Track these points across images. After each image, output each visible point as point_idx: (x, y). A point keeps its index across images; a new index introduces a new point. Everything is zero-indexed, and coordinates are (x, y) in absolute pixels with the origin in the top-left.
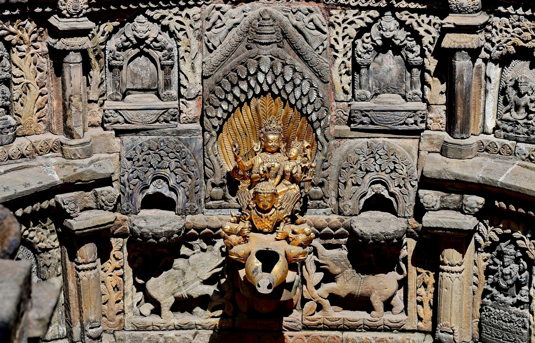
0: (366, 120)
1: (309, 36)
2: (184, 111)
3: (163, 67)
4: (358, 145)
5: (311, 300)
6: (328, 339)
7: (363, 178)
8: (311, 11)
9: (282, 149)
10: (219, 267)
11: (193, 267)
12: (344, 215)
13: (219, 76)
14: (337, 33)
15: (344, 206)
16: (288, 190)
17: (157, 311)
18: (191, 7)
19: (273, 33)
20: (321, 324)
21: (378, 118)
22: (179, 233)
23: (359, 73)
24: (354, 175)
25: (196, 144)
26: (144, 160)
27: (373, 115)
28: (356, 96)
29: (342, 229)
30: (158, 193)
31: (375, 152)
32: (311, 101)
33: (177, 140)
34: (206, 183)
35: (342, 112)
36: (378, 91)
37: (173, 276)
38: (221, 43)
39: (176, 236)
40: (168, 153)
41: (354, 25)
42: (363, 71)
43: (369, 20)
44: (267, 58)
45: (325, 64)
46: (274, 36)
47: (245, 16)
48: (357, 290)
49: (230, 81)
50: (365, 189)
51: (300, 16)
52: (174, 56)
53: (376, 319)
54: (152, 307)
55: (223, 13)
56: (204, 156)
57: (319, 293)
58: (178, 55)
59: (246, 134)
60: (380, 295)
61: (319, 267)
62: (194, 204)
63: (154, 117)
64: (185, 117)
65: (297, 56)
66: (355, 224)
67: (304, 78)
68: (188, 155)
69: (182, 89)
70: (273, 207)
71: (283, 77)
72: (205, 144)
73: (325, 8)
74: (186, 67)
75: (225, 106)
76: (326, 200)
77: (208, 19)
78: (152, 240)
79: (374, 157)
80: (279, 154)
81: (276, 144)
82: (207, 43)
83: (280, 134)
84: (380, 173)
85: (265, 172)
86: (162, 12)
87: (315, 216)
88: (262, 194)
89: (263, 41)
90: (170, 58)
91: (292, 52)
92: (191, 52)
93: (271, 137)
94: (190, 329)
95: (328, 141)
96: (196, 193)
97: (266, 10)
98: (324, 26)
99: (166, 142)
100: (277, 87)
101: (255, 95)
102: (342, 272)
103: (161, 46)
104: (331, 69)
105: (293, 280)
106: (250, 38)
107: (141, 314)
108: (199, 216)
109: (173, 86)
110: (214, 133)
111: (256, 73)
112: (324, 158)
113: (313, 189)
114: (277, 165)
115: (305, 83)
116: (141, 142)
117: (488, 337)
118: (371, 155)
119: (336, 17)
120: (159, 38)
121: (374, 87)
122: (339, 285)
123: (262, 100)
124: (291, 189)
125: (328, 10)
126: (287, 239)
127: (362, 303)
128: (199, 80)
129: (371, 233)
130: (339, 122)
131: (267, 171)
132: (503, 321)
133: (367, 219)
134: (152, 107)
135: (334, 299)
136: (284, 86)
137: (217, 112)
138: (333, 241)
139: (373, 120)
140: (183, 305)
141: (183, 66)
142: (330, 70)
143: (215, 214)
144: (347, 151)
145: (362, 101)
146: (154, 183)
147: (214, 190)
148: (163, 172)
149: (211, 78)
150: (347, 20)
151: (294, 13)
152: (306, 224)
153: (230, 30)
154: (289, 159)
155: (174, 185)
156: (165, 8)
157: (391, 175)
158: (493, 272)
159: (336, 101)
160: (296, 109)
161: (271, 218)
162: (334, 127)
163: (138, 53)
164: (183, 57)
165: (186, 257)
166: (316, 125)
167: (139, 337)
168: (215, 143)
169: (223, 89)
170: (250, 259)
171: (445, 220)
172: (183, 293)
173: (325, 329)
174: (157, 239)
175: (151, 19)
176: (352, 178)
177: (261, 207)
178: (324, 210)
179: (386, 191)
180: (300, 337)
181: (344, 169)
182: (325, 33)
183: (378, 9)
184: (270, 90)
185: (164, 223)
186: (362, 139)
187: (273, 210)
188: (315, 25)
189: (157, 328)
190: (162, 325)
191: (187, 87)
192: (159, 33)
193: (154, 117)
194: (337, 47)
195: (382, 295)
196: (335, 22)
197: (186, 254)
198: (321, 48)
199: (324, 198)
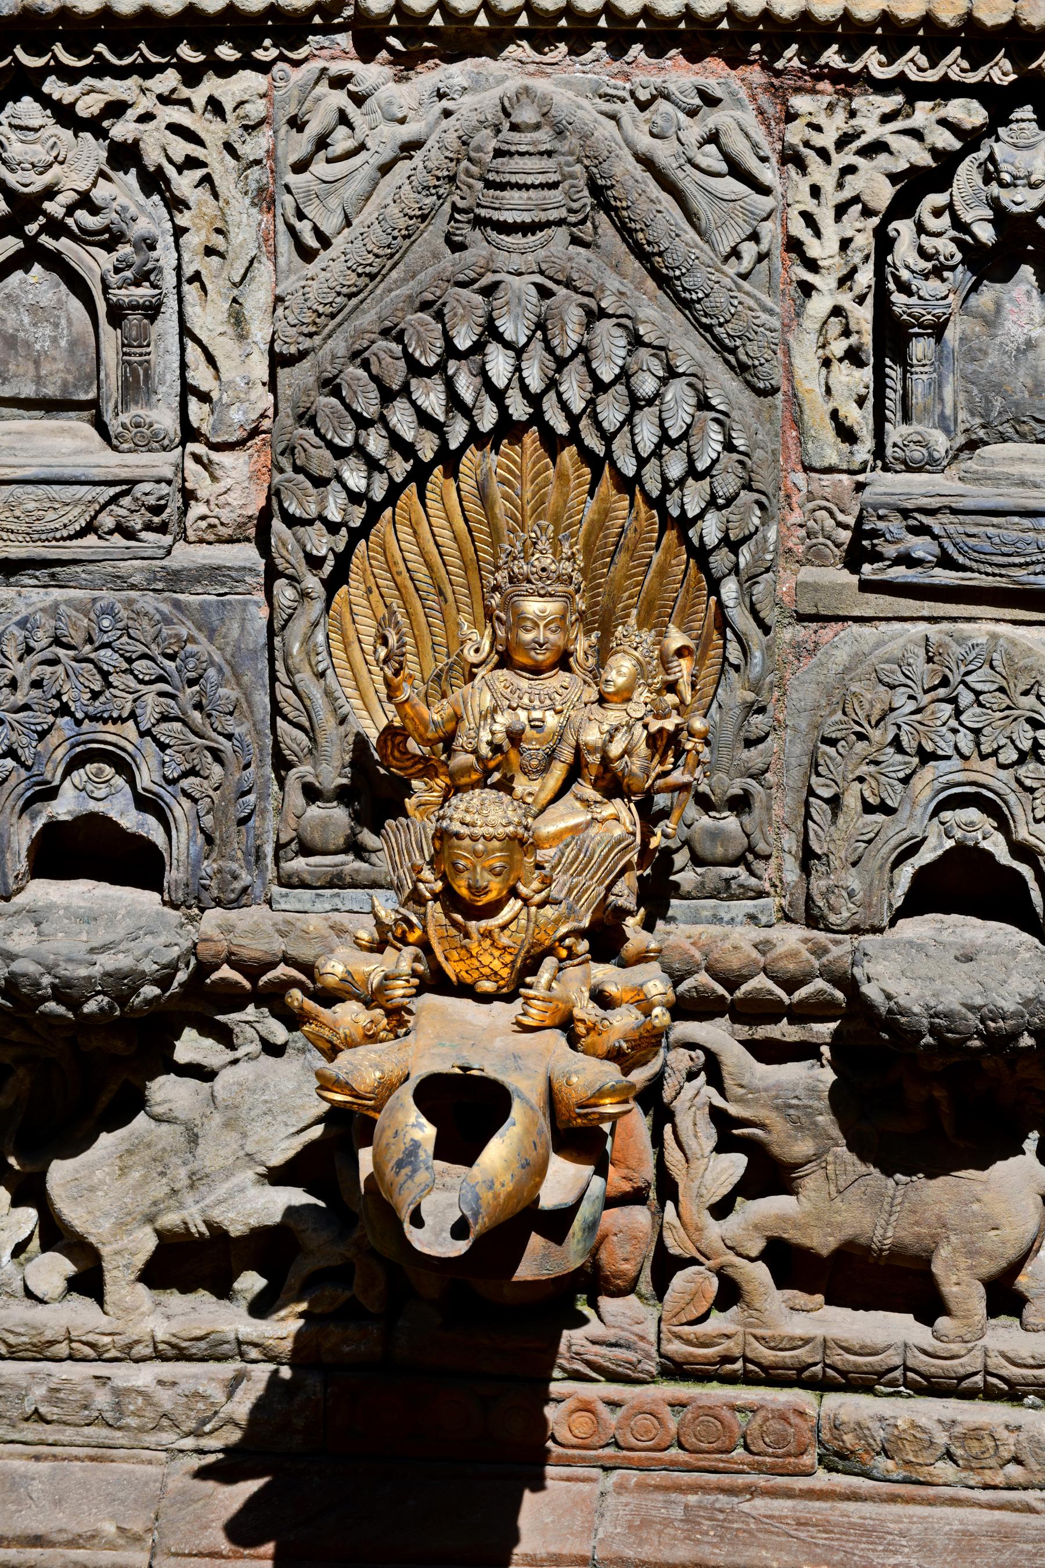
0: (921, 547)
1: (700, 203)
2: (200, 494)
3: (117, 315)
4: (887, 648)
5: (693, 1261)
6: (759, 1419)
7: (906, 781)
8: (711, 101)
9: (580, 655)
10: (317, 1122)
11: (230, 1113)
12: (828, 929)
13: (334, 357)
14: (815, 191)
15: (830, 890)
16: (588, 825)
17: (88, 1282)
18: (226, 70)
19: (554, 186)
20: (733, 1360)
21: (971, 541)
22: (164, 981)
23: (903, 360)
24: (872, 768)
25: (243, 628)
26: (37, 684)
27: (951, 529)
28: (889, 451)
29: (819, 984)
30: (93, 816)
31: (955, 678)
32: (701, 466)
33: (166, 608)
34: (281, 782)
35: (831, 514)
36: (981, 433)
37: (149, 1146)
38: (349, 224)
39: (150, 991)
40: (130, 661)
41: (882, 158)
42: (920, 348)
43: (946, 140)
44: (524, 287)
45: (764, 317)
46: (556, 196)
47: (447, 114)
48: (879, 1232)
49: (374, 378)
50: (915, 829)
51: (667, 118)
52: (160, 270)
53: (955, 1348)
54: (69, 1268)
55: (358, 99)
56: (273, 678)
57: (728, 1235)
58: (179, 269)
59: (441, 593)
60: (971, 1253)
61: (728, 1133)
62: (235, 866)
63: (76, 511)
64: (203, 518)
65: (651, 284)
66: (870, 968)
67: (672, 373)
68: (212, 672)
69: (193, 403)
70: (514, 893)
71: (587, 363)
72: (276, 626)
73: (771, 88)
74: (208, 318)
75: (356, 480)
76: (758, 866)
77: (297, 124)
78: (51, 1006)
79: (953, 700)
80: (564, 677)
81: (552, 637)
82: (293, 220)
83: (569, 598)
84: (975, 763)
85: (496, 748)
86: (114, 89)
87: (715, 930)
88: (467, 842)
89: (509, 217)
90: (143, 277)
91: (633, 265)
92: (230, 256)
93: (533, 606)
94: (219, 1359)
95: (766, 629)
96: (243, 821)
97: (527, 90)
98: (764, 160)
99: (124, 614)
100: (564, 406)
101: (475, 437)
102: (817, 1156)
103: (107, 229)
104: (790, 338)
105: (569, 1199)
106: (461, 204)
107: (29, 1294)
108: (255, 914)
109: (162, 389)
110: (312, 582)
111: (478, 348)
112: (750, 696)
113: (705, 821)
114: (552, 721)
115: (677, 392)
116: (24, 613)
118: (942, 692)
119: (810, 125)
120: (101, 192)
121: (962, 415)
122: (807, 1205)
123: (507, 456)
124: (603, 821)
125: (779, 94)
126: (567, 1024)
127: (898, 1280)
128: (260, 369)
129: (928, 1008)
130: (819, 555)
131: (506, 744)
133: (920, 948)
134: (67, 473)
135: (789, 1264)
136: (591, 403)
137: (322, 502)
138: (784, 1031)
139: (951, 550)
140: (187, 1262)
141: (198, 309)
142: (786, 344)
143: (319, 907)
144: (847, 670)
145: (910, 469)
146: (79, 776)
147: (315, 811)
148: (108, 734)
149: (306, 364)
150: (857, 136)
151: (643, 106)
152: (655, 966)
153: (385, 169)
154: (602, 700)
155: (156, 788)
156: (121, 73)
157: (1022, 771)
159: (808, 469)
160: (639, 497)
161: (504, 940)
162: (795, 573)
163: (18, 252)
164: (197, 277)
165: (202, 1073)
166: (720, 561)
167: (15, 1386)
168: (315, 624)
169: (348, 407)
170: (392, 1109)
172: (190, 1215)
173: (749, 1380)
174: (75, 1004)
175: (65, 115)
176: (861, 779)
177: (464, 892)
178: (749, 906)
179: (1000, 838)
180: (647, 1408)
181: (832, 742)
182: (764, 190)
183: (983, 92)
184: (537, 418)
185: (109, 938)
186: (907, 625)
187: (513, 906)
188: (728, 158)
189: (88, 1351)
190: (107, 1340)
191: (215, 395)
192: (102, 174)
193: (76, 511)
194: (814, 249)
195: (979, 1252)
196: (807, 144)
197: (205, 1062)
198: (749, 250)
199: (750, 857)
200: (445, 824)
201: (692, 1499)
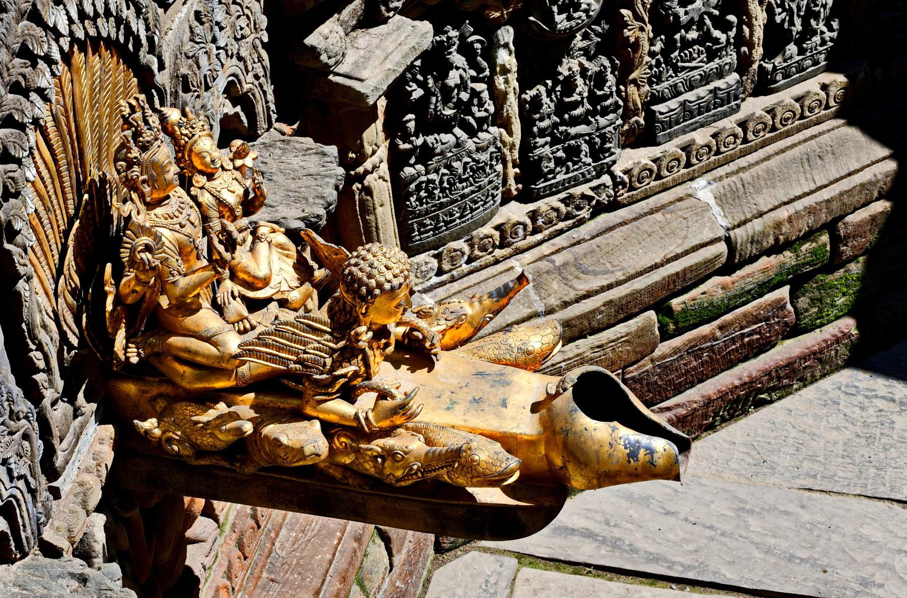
117: (428, 237)
171: (396, 57)
200: (387, 286)
201: (265, 575)
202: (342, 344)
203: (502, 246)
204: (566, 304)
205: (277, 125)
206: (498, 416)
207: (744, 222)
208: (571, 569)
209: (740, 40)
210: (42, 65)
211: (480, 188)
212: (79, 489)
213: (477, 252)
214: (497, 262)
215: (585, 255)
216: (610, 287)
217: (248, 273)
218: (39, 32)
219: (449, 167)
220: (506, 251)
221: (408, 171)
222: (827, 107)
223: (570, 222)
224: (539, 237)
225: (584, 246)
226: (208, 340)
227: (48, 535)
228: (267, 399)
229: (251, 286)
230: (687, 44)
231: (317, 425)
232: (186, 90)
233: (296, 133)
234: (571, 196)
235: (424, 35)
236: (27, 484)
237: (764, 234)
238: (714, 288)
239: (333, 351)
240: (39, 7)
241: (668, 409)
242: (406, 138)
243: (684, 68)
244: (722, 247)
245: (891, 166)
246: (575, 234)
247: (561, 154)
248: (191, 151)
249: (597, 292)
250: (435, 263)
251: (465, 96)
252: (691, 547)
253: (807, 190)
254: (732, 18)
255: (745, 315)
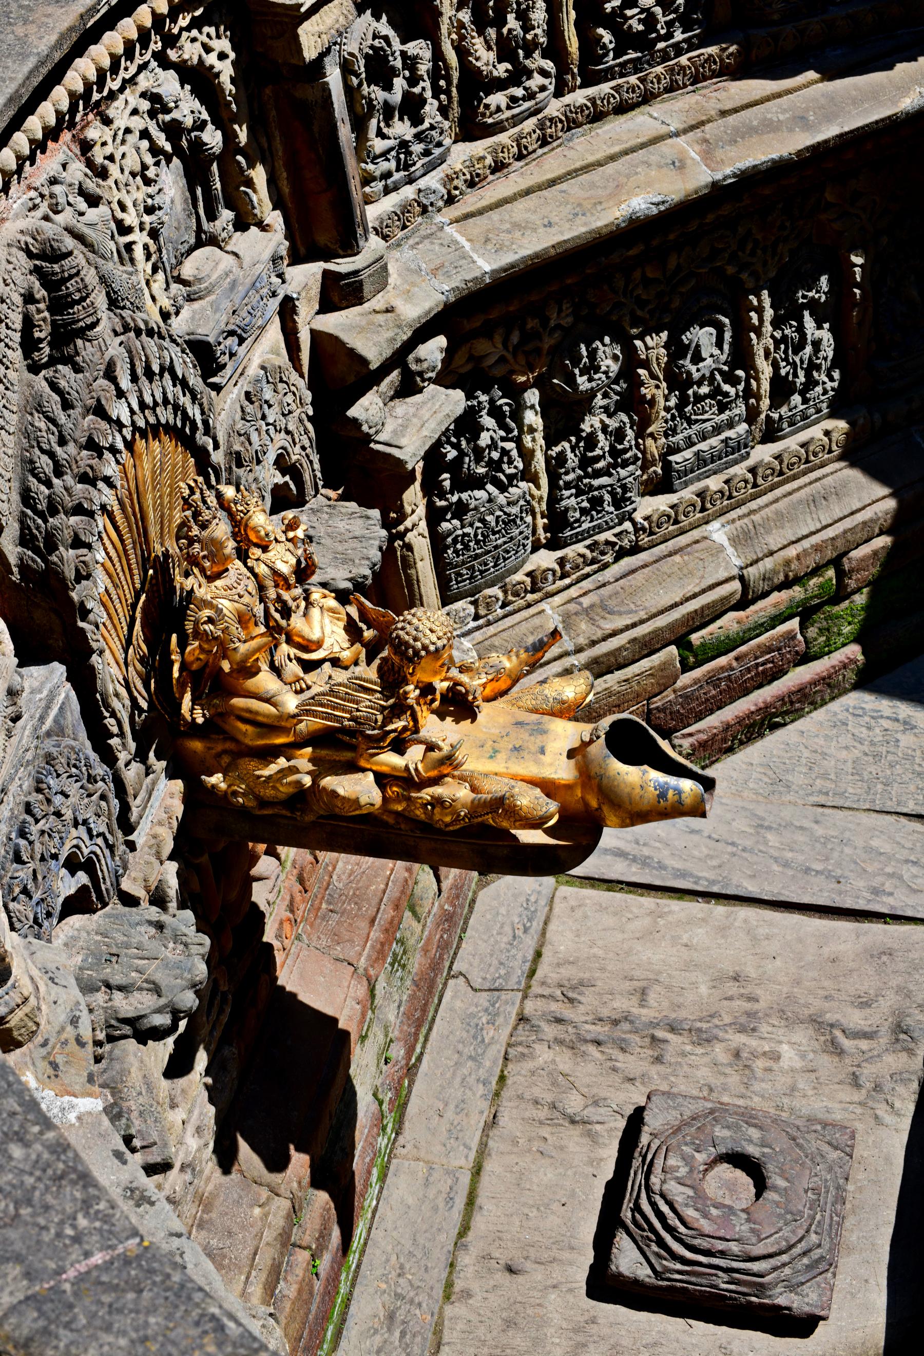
106: (42, 335)
132: (494, 533)
158: (455, 466)
171: (432, 424)
200: (432, 648)
201: (324, 906)
202: (391, 701)
203: (533, 591)
204: (593, 643)
205: (323, 491)
206: (537, 762)
207: (756, 561)
208: (605, 886)
209: (748, 393)
210: (107, 455)
211: (512, 539)
212: (153, 841)
213: (510, 598)
214: (529, 606)
215: (610, 597)
216: (634, 625)
217: (303, 637)
218: (104, 425)
219: (482, 521)
220: (536, 596)
221: (445, 526)
222: (830, 451)
223: (595, 566)
224: (567, 581)
225: (609, 588)
226: (267, 700)
227: (126, 885)
228: (324, 753)
229: (306, 649)
230: (699, 398)
231: (371, 776)
232: (240, 465)
233: (342, 498)
234: (596, 543)
235: (457, 403)
236: (106, 840)
237: (775, 572)
238: (730, 622)
239: (383, 708)
240: (103, 402)
241: (691, 735)
242: (442, 497)
243: (697, 421)
244: (736, 585)
245: (891, 504)
246: (601, 577)
247: (585, 504)
248: (246, 525)
249: (622, 631)
250: (471, 609)
251: (495, 455)
252: (715, 863)
253: (813, 529)
254: (740, 373)
255: (759, 646)
